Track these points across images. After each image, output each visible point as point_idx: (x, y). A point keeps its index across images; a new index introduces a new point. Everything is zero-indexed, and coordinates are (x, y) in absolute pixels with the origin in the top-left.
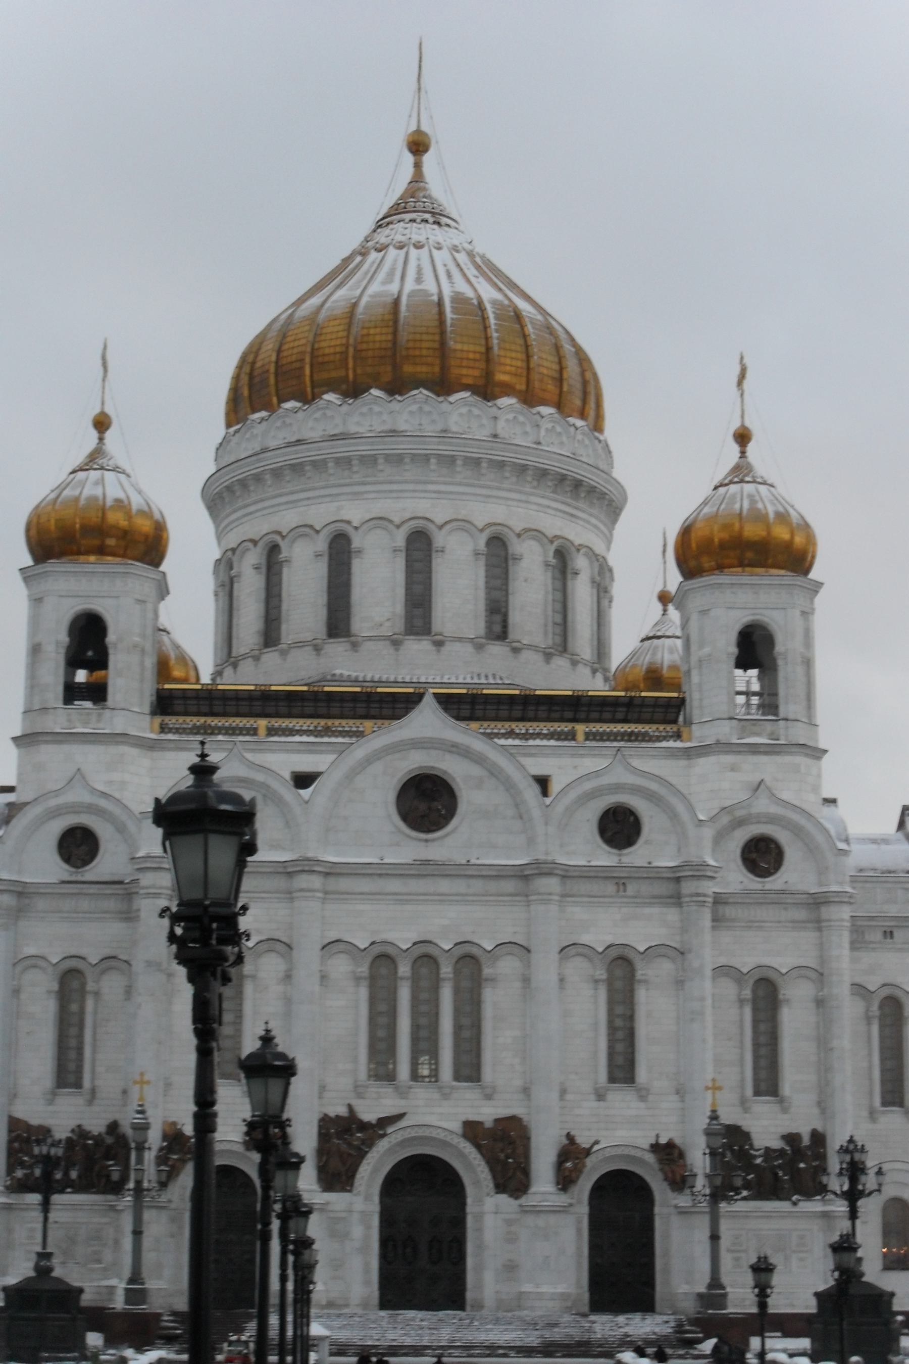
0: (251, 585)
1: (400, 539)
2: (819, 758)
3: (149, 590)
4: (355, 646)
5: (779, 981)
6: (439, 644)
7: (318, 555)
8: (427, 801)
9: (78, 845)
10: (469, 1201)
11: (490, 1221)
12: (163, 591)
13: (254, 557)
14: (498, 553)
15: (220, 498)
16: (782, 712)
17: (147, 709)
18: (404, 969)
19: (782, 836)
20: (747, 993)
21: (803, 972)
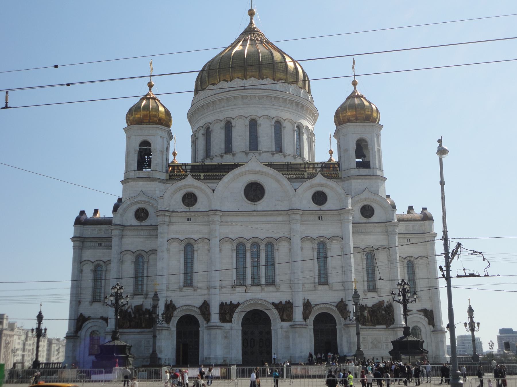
1: (247, 122)
2: (385, 181)
3: (165, 135)
7: (221, 128)
8: (254, 192)
9: (141, 214)
10: (272, 325)
11: (280, 331)
12: (171, 137)
13: (202, 131)
14: (278, 125)
15: (192, 116)
16: (372, 166)
17: (164, 171)
18: (248, 246)
19: (374, 206)
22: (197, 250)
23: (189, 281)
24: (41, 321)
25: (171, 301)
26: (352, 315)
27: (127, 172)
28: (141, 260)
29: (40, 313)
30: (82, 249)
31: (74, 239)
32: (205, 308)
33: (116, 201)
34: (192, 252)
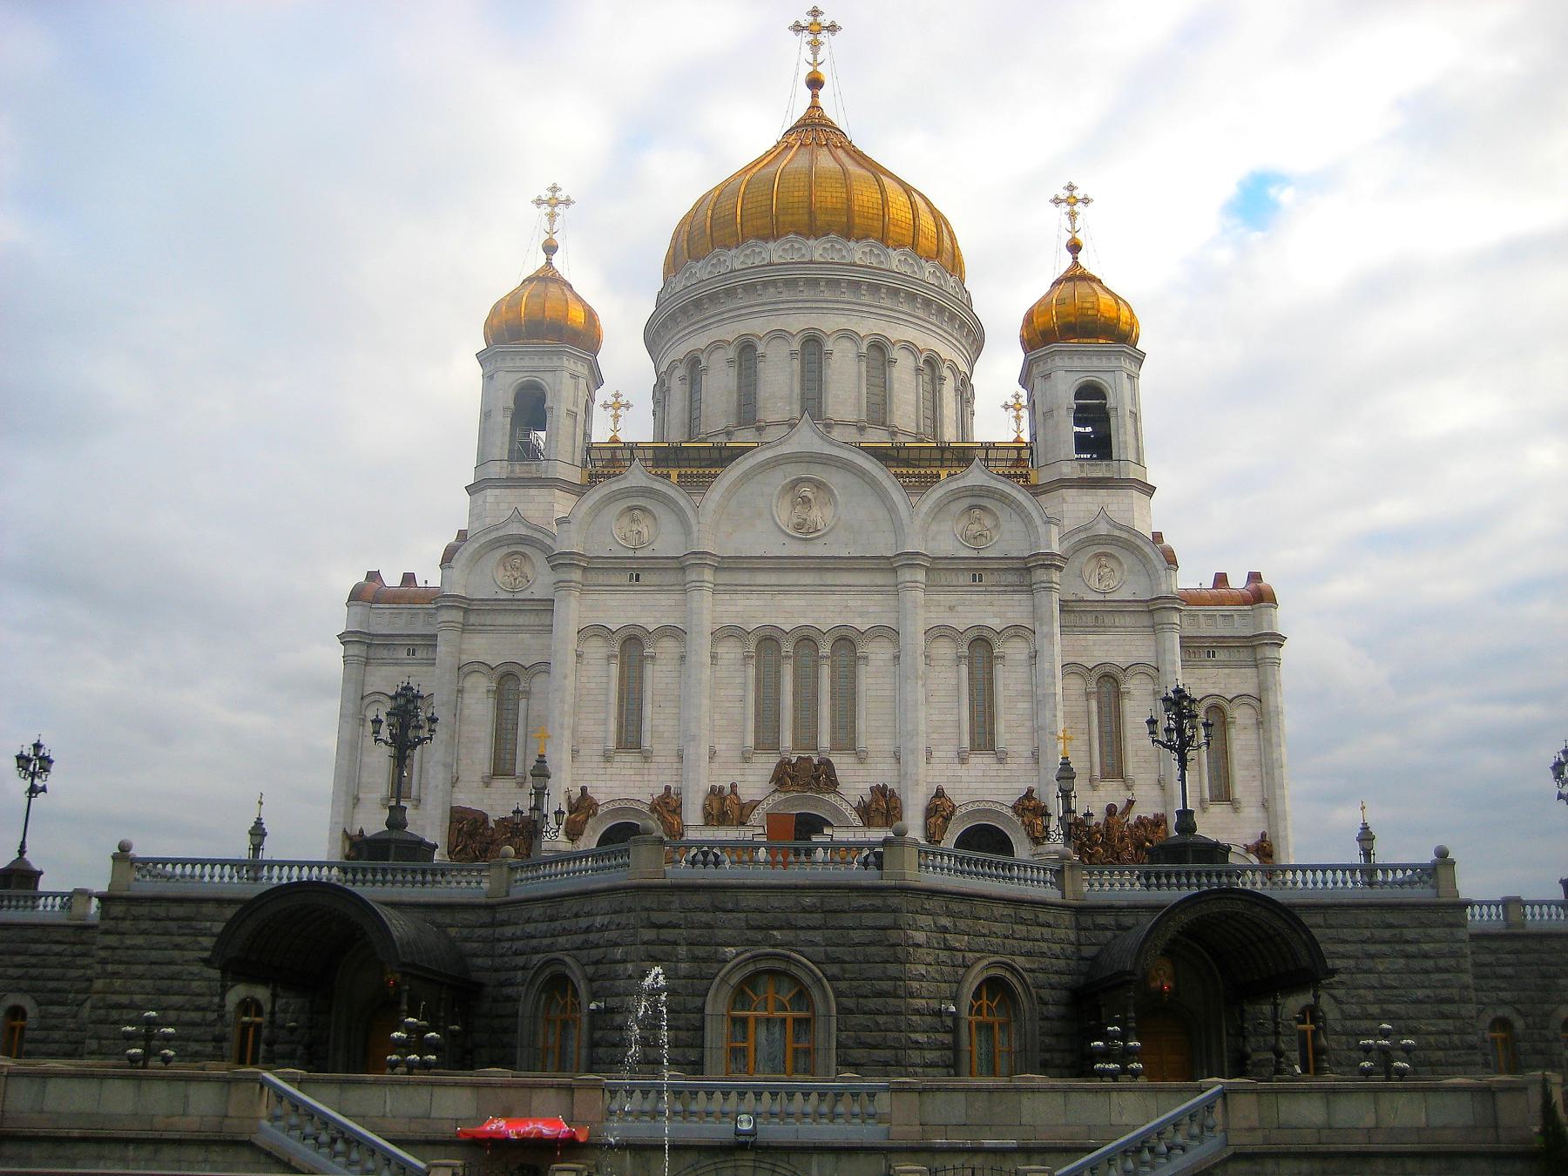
0: (678, 391)
1: (796, 346)
3: (582, 369)
4: (759, 429)
5: (1121, 676)
6: (828, 426)
13: (681, 371)
15: (656, 335)
18: (788, 648)
20: (1093, 687)
21: (1141, 669)
22: (653, 658)
23: (630, 738)
24: (261, 843)
25: (584, 789)
26: (1054, 823)
27: (482, 463)
28: (510, 685)
29: (259, 823)
30: (366, 664)
31: (345, 639)
32: (668, 805)
33: (452, 538)
34: (643, 659)
